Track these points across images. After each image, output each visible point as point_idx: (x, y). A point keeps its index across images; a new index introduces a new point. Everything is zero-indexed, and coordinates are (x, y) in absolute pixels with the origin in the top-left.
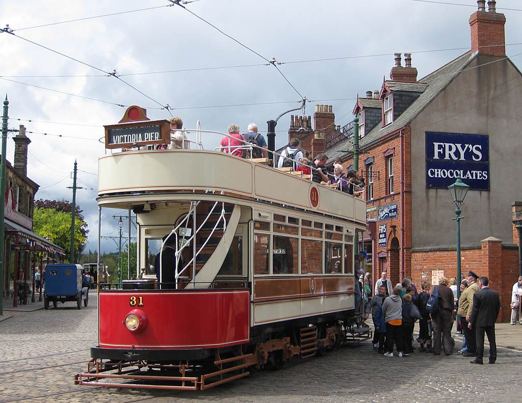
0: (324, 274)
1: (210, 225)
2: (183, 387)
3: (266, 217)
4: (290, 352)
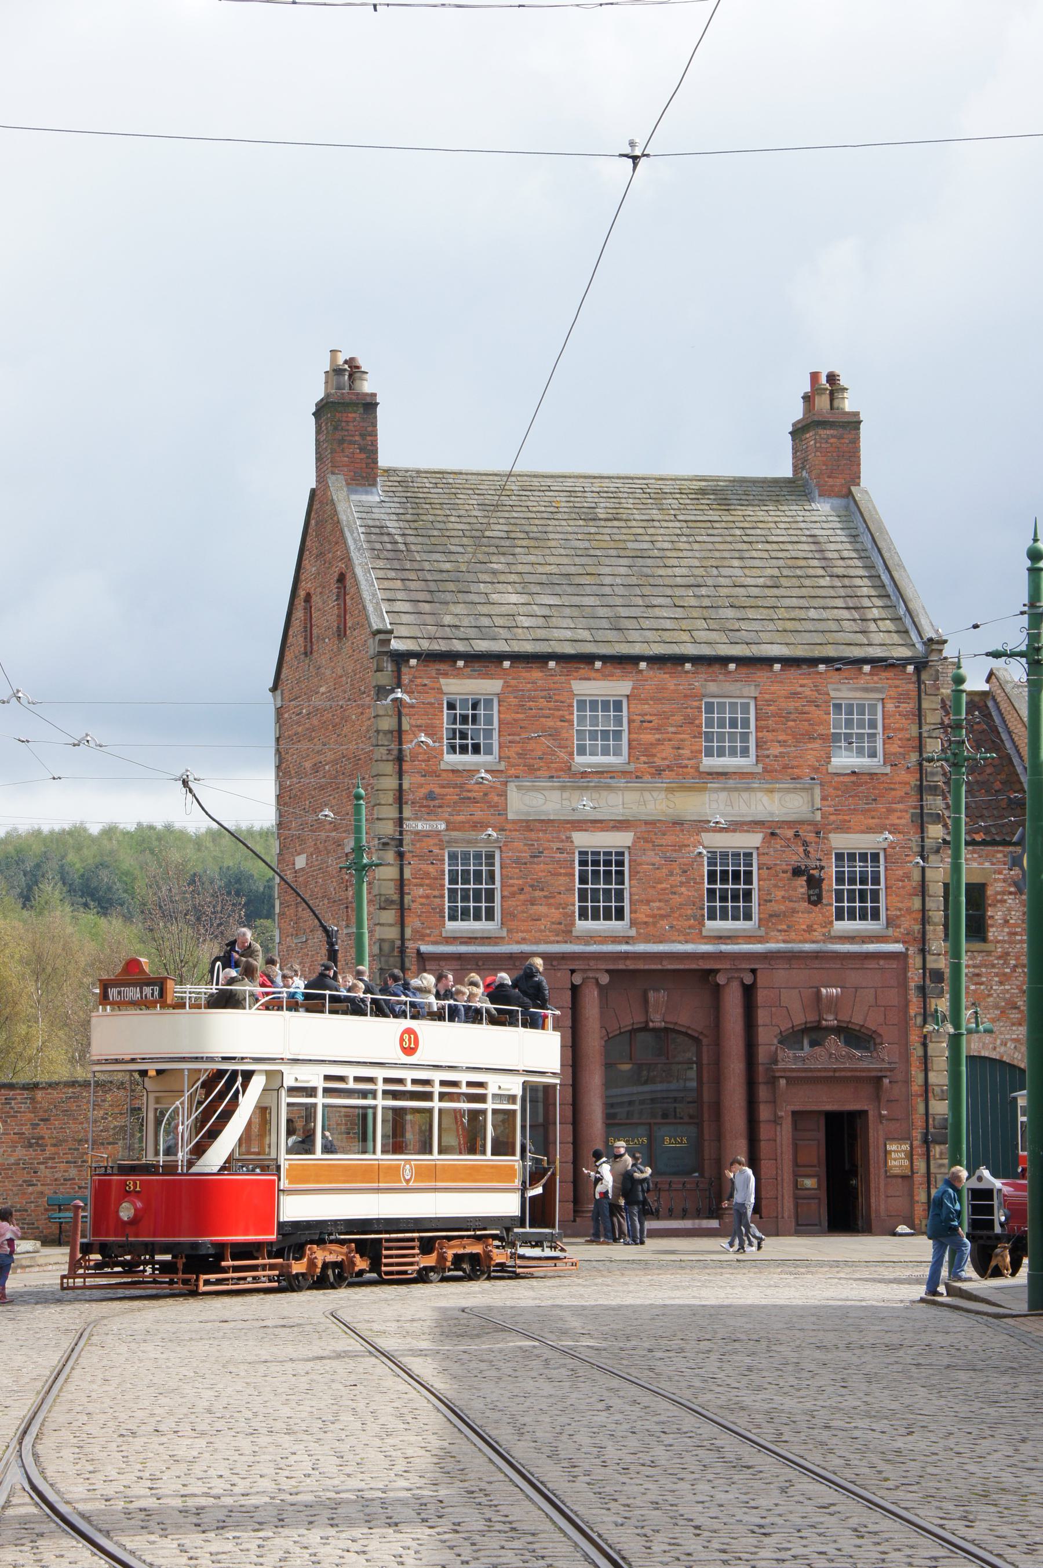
1: (221, 1096)
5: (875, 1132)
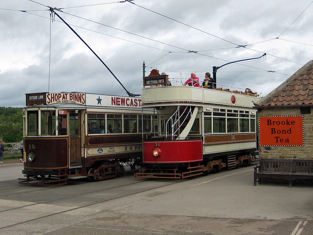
0: (239, 133)
1: (185, 114)
2: (175, 177)
3: (209, 110)
4: (222, 166)
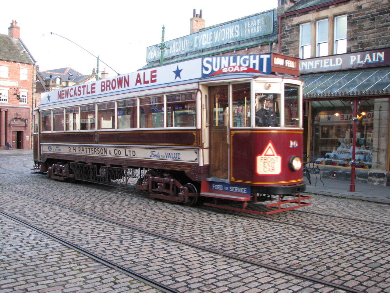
5: (25, 134)
